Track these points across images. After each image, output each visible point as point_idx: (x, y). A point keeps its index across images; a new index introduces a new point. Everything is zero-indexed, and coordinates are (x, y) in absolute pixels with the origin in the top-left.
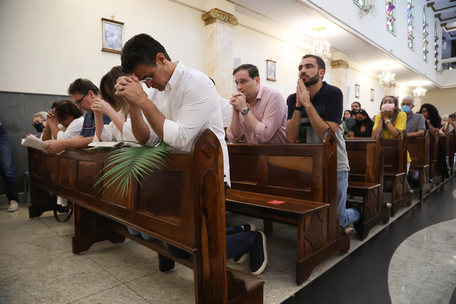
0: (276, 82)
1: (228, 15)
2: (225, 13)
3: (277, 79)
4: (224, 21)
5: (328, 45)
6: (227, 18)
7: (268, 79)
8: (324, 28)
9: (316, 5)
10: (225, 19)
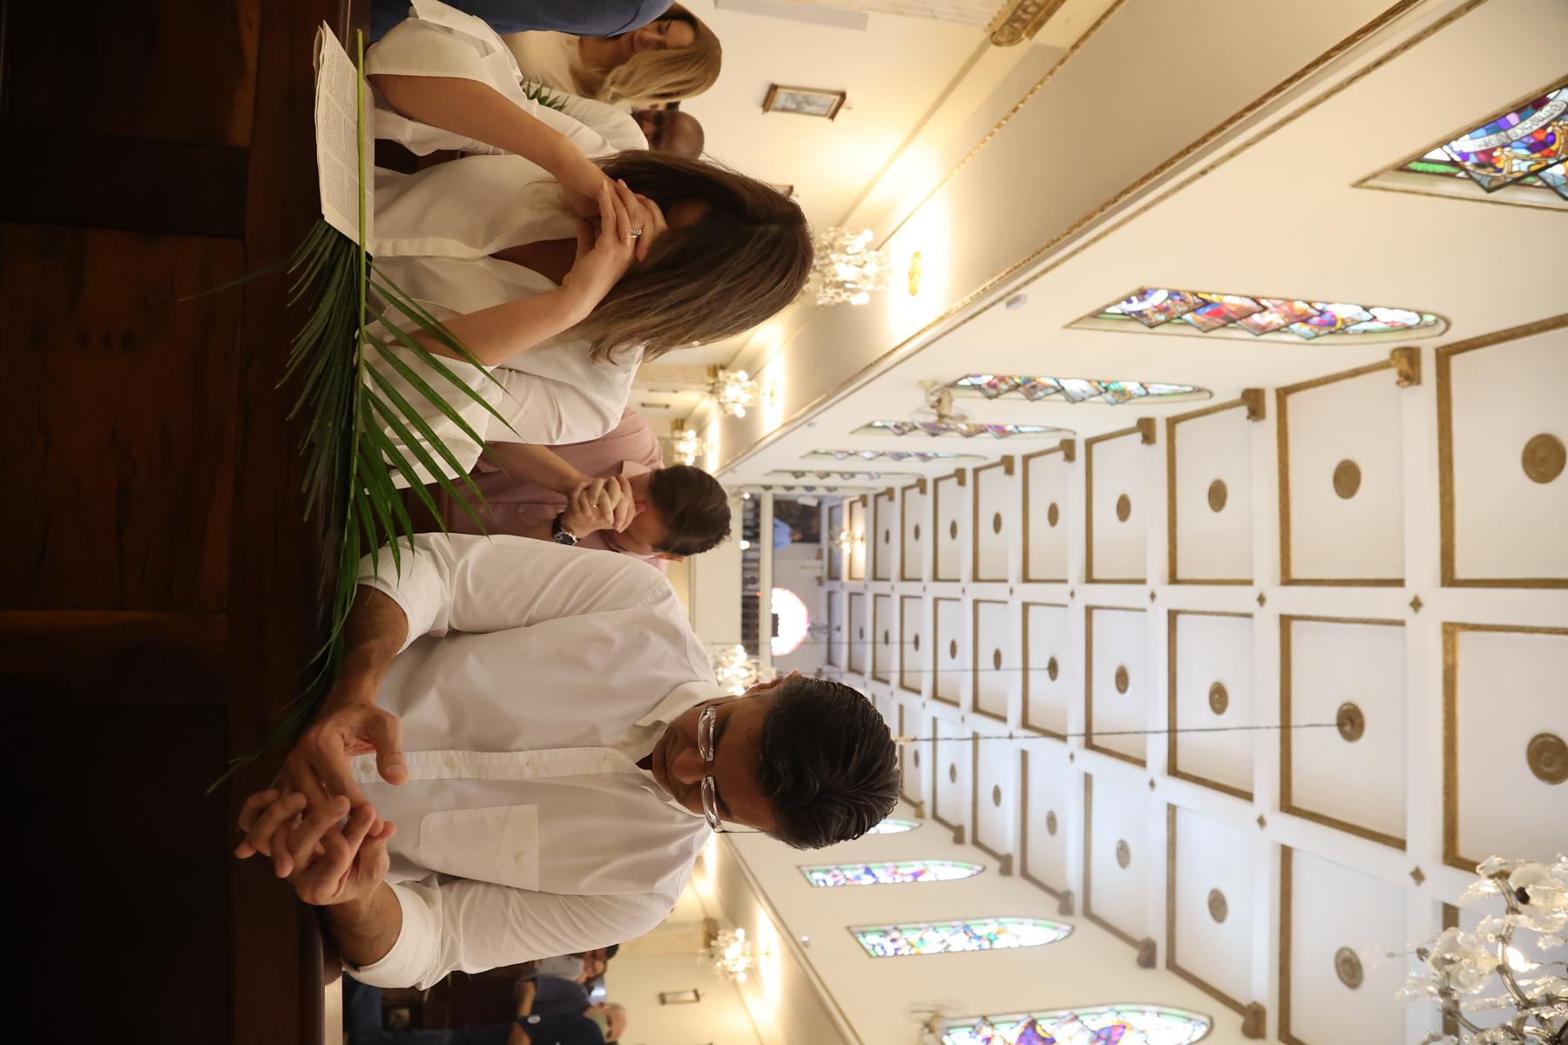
0: (761, 110)
1: (1037, 19)
2: (1050, 13)
3: (771, 114)
4: (1020, 6)
5: (858, 300)
6: (1024, 16)
7: (774, 88)
8: (913, 292)
9: (986, 309)
10: (1025, 11)
